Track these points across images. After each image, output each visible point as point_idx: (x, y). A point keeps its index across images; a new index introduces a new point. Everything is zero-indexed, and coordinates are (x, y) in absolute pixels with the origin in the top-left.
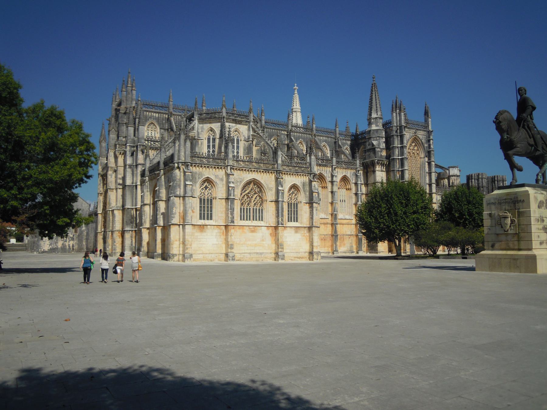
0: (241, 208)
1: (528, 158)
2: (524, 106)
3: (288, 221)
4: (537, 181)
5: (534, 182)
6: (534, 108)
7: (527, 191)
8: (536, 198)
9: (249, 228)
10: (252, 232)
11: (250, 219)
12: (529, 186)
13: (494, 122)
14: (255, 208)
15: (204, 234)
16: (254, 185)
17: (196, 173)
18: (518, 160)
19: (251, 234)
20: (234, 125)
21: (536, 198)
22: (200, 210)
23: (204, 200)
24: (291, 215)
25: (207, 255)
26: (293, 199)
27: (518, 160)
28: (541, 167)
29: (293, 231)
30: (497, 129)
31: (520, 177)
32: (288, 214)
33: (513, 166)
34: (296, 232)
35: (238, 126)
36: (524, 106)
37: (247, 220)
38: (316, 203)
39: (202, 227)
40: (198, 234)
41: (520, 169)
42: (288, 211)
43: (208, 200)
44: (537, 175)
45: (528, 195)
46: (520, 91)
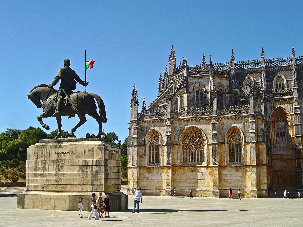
0: (184, 153)
3: (230, 160)
9: (190, 169)
10: (192, 171)
11: (192, 161)
14: (197, 151)
15: (151, 174)
16: (195, 132)
17: (144, 127)
19: (191, 173)
20: (197, 81)
22: (150, 156)
23: (153, 147)
24: (234, 155)
25: (153, 190)
26: (235, 141)
29: (233, 170)
32: (230, 154)
34: (237, 171)
35: (201, 80)
37: (189, 161)
38: (253, 143)
39: (149, 169)
40: (146, 174)
42: (230, 152)
43: (156, 147)
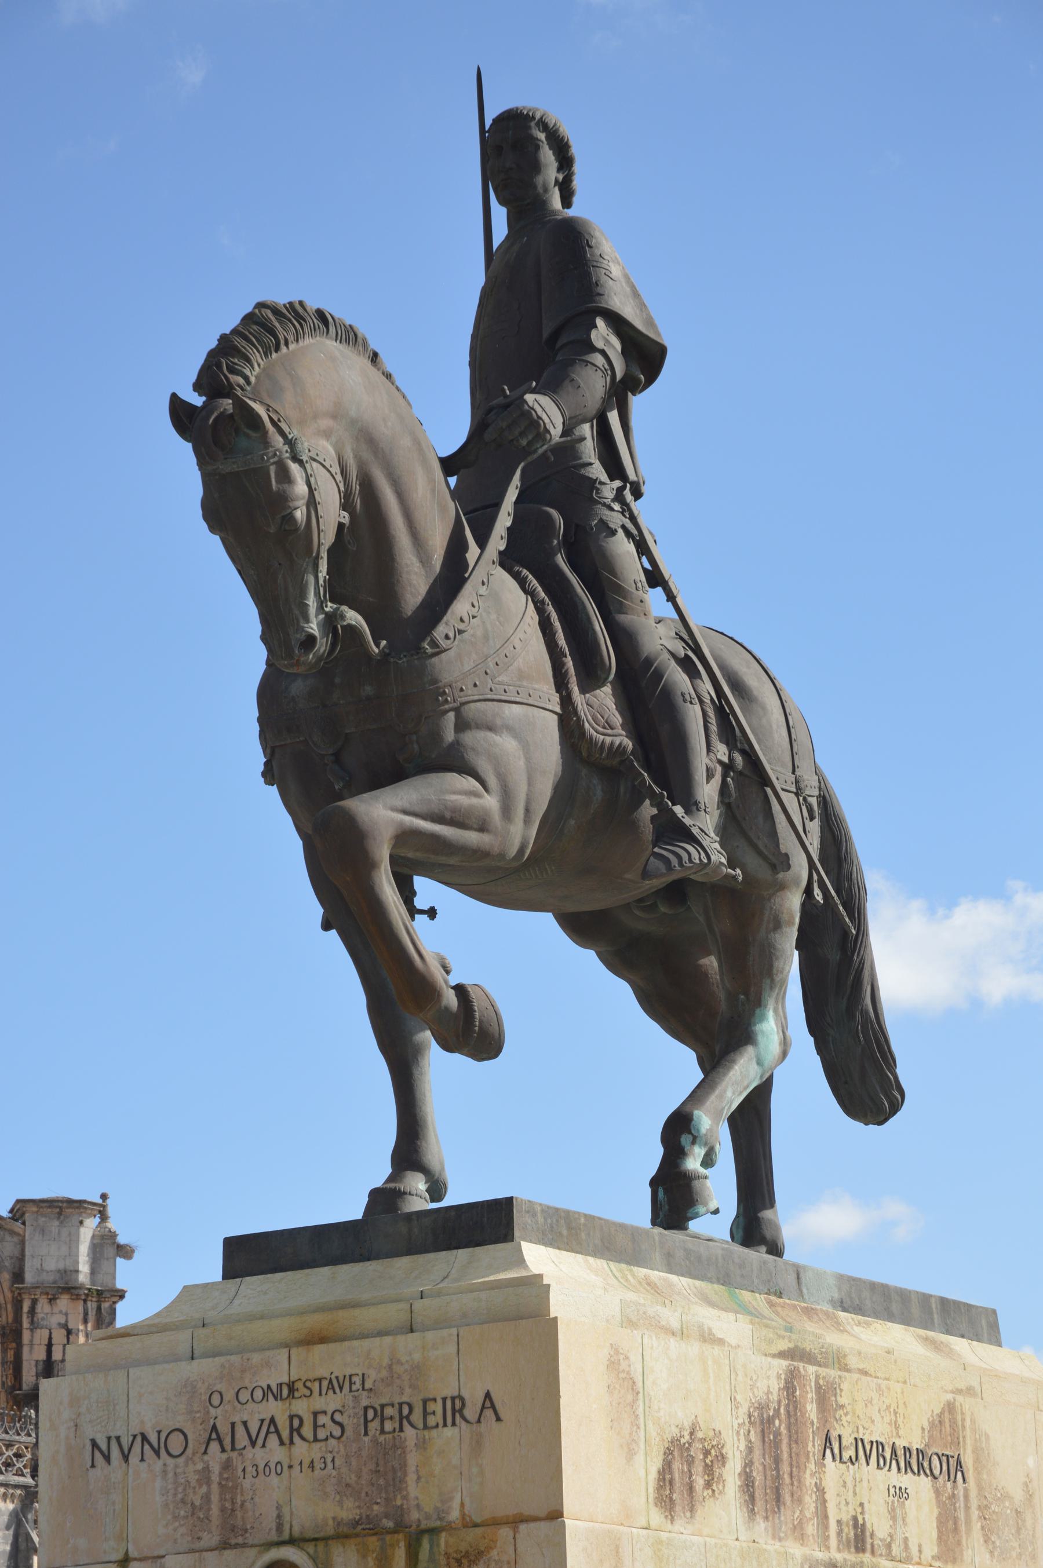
1: (580, 927)
2: (544, 304)
4: (673, 1197)
5: (636, 1208)
6: (645, 358)
7: (536, 1288)
8: (626, 1384)
12: (569, 1231)
13: (182, 416)
18: (457, 934)
21: (626, 1384)
27: (457, 934)
28: (714, 1060)
30: (219, 512)
31: (484, 1133)
33: (416, 1015)
36: (544, 304)
41: (474, 1033)
44: (678, 1128)
45: (547, 1331)
46: (517, 153)
